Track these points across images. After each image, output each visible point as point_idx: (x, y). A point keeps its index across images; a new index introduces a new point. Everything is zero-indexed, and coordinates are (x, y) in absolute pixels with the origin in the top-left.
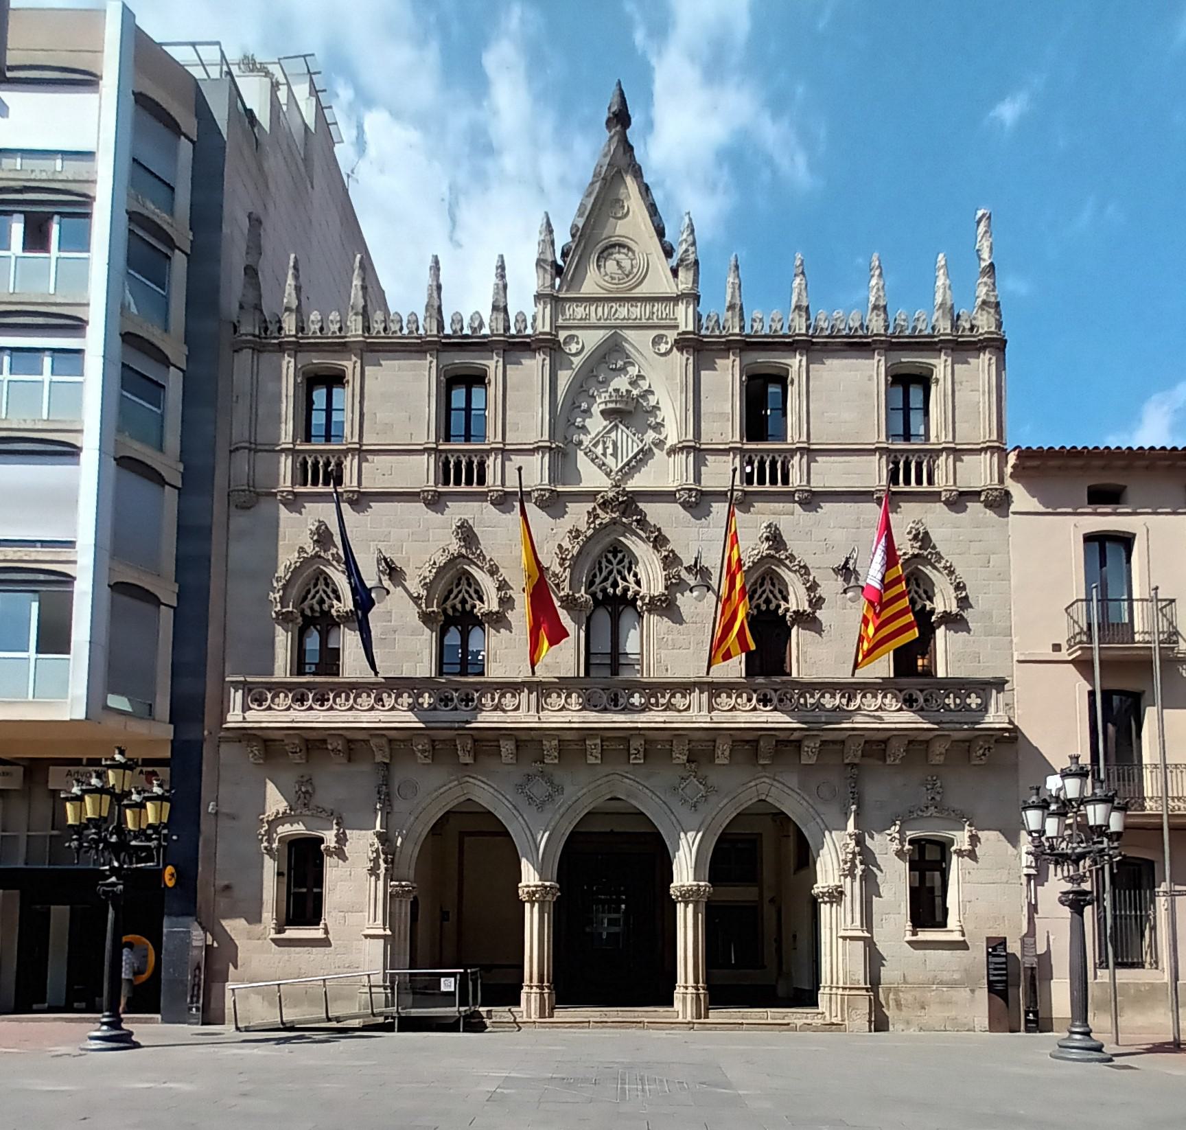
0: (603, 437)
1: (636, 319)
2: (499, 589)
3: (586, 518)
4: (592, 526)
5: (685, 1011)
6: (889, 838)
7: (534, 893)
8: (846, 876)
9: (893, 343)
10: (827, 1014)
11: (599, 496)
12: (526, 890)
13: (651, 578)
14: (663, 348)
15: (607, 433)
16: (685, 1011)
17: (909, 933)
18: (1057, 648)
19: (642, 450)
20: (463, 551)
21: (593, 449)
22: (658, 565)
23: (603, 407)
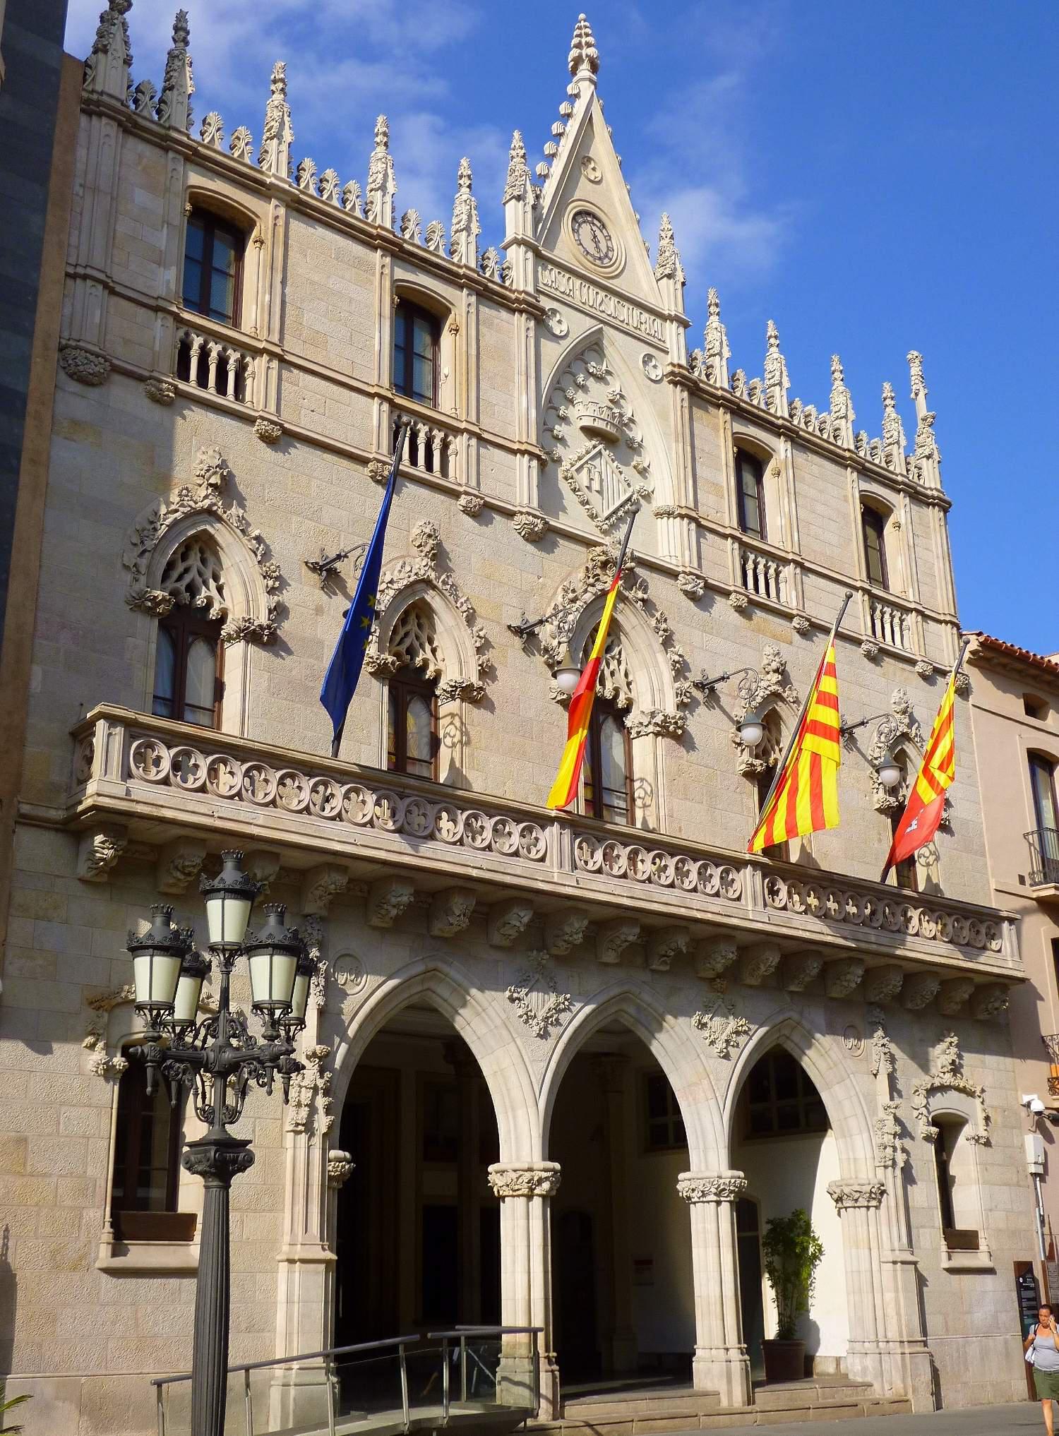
0: (586, 462)
1: (622, 322)
2: (479, 650)
3: (581, 575)
4: (590, 589)
5: (730, 1393)
6: (916, 1113)
7: (540, 1181)
8: (886, 1167)
9: (865, 468)
10: (877, 1386)
11: (598, 549)
12: (528, 1175)
13: (656, 687)
14: (656, 374)
15: (590, 459)
16: (730, 1393)
17: (944, 1256)
18: (1022, 880)
19: (629, 499)
20: (433, 575)
21: (575, 474)
22: (668, 674)
23: (587, 422)
